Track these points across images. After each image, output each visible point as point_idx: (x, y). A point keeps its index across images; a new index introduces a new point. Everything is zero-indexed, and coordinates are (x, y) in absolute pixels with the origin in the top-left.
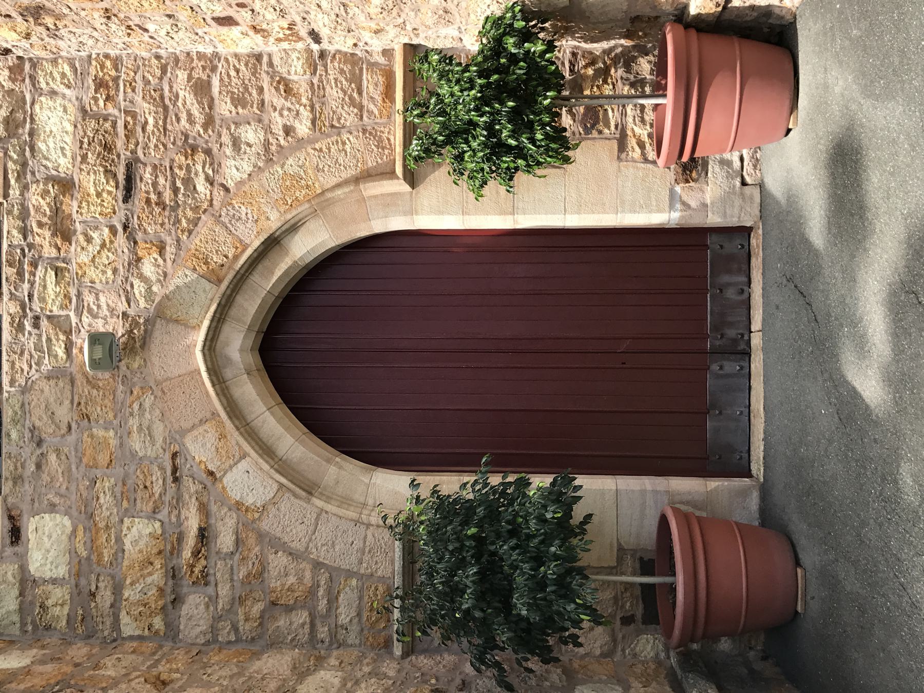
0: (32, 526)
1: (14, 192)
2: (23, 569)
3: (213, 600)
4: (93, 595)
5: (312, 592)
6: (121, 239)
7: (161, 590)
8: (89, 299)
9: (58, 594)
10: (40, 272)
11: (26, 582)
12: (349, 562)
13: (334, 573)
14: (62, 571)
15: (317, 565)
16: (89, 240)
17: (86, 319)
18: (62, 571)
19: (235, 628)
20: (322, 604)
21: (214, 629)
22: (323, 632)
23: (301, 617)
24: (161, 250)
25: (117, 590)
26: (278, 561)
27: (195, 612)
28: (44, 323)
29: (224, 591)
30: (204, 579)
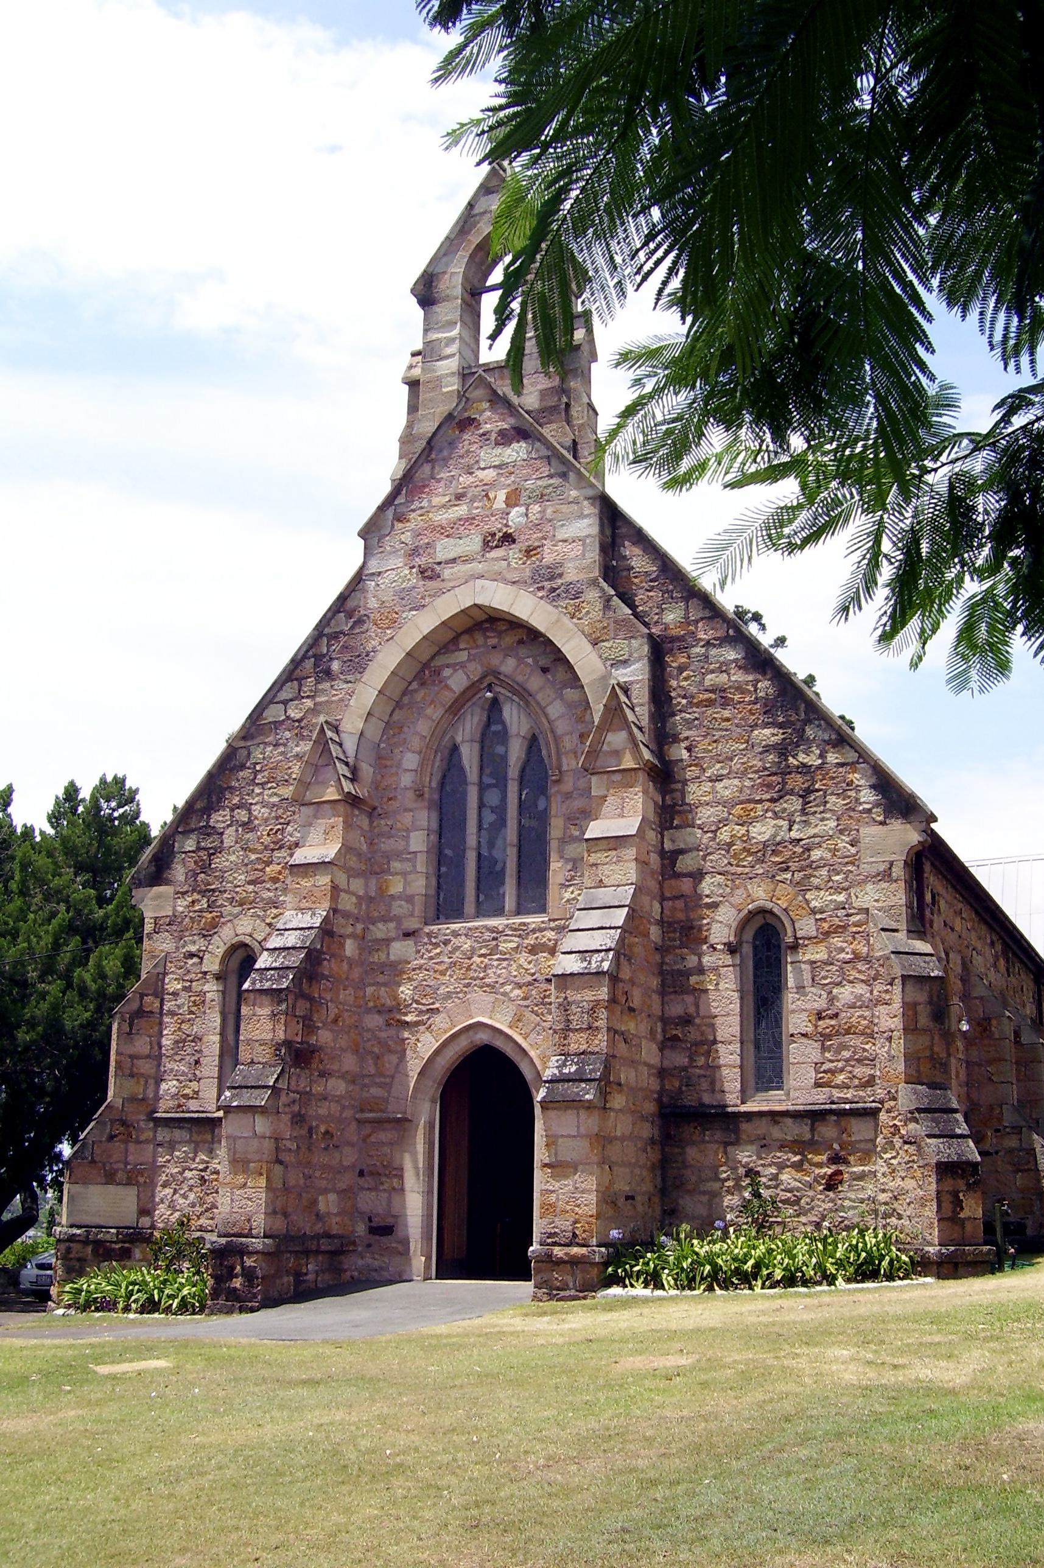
0: (410, 942)
1: (552, 924)
2: (393, 939)
3: (380, 1030)
4: (382, 973)
5: (382, 1075)
6: (530, 978)
7: (383, 1005)
8: (505, 964)
9: (383, 957)
10: (516, 939)
11: (387, 941)
12: (395, 1092)
13: (391, 1085)
14: (392, 958)
15: (393, 1077)
16: (530, 963)
17: (495, 963)
18: (392, 958)
19: (369, 1040)
20: (377, 1080)
21: (368, 1030)
22: (367, 1081)
23: (373, 1072)
24: (525, 999)
25: (385, 984)
26: (394, 1059)
27: (374, 1021)
28: (494, 943)
29: (383, 1035)
30: (389, 1025)
